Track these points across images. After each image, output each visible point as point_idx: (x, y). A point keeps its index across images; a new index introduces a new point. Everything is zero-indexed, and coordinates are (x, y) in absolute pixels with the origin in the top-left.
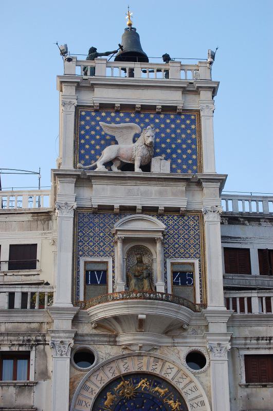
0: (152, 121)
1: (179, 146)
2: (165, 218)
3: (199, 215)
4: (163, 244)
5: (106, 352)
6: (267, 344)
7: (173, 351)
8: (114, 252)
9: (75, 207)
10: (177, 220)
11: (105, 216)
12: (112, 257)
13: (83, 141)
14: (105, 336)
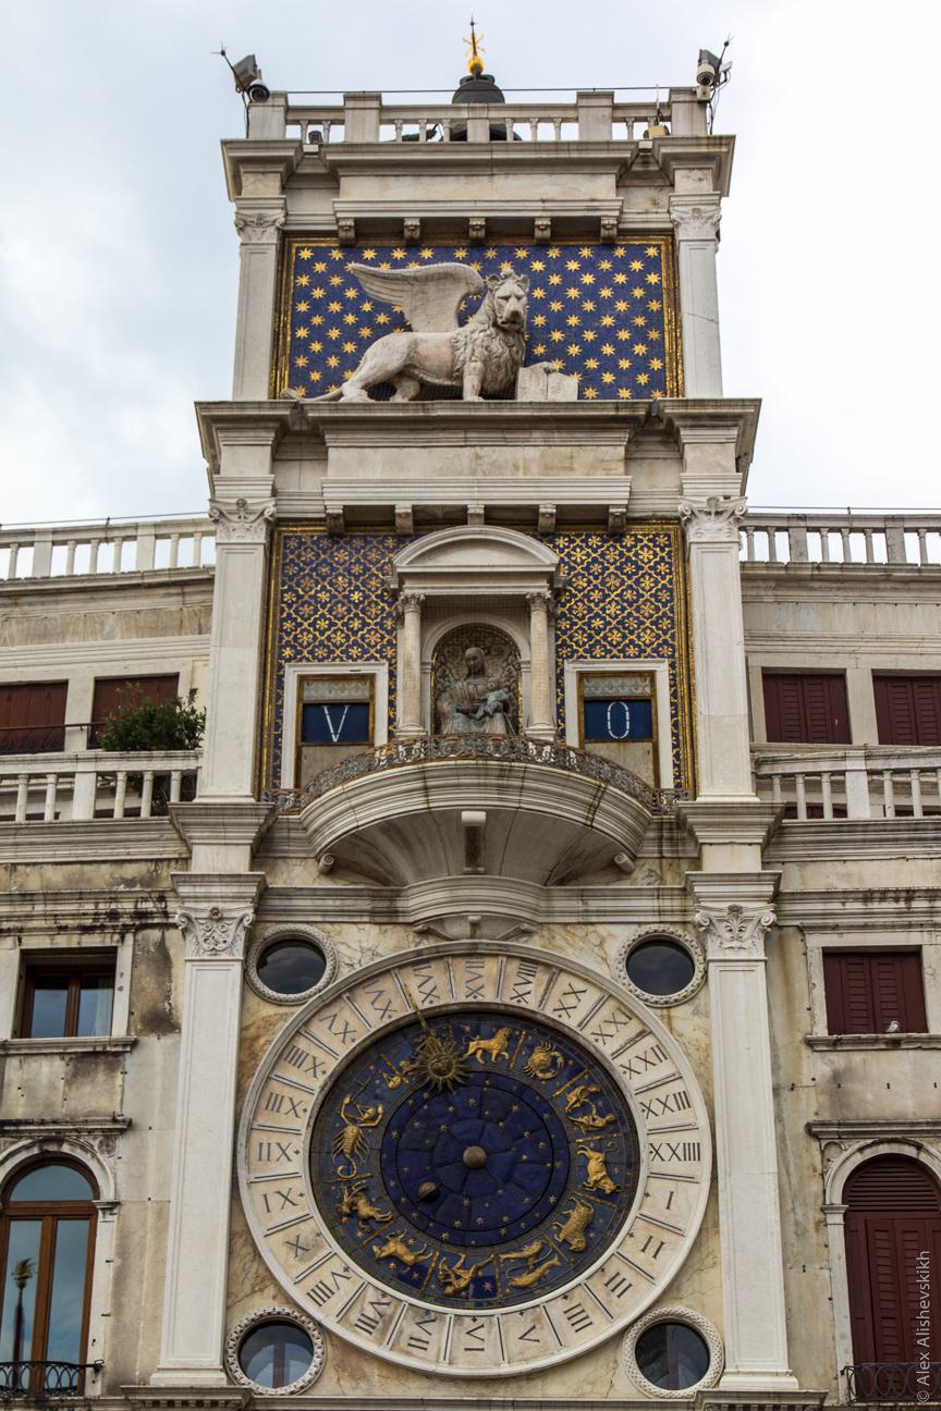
1: (607, 335)
2: (561, 542)
5: (363, 945)
7: (585, 939)
8: (394, 646)
11: (367, 542)
12: (389, 660)
13: (302, 333)
14: (357, 894)
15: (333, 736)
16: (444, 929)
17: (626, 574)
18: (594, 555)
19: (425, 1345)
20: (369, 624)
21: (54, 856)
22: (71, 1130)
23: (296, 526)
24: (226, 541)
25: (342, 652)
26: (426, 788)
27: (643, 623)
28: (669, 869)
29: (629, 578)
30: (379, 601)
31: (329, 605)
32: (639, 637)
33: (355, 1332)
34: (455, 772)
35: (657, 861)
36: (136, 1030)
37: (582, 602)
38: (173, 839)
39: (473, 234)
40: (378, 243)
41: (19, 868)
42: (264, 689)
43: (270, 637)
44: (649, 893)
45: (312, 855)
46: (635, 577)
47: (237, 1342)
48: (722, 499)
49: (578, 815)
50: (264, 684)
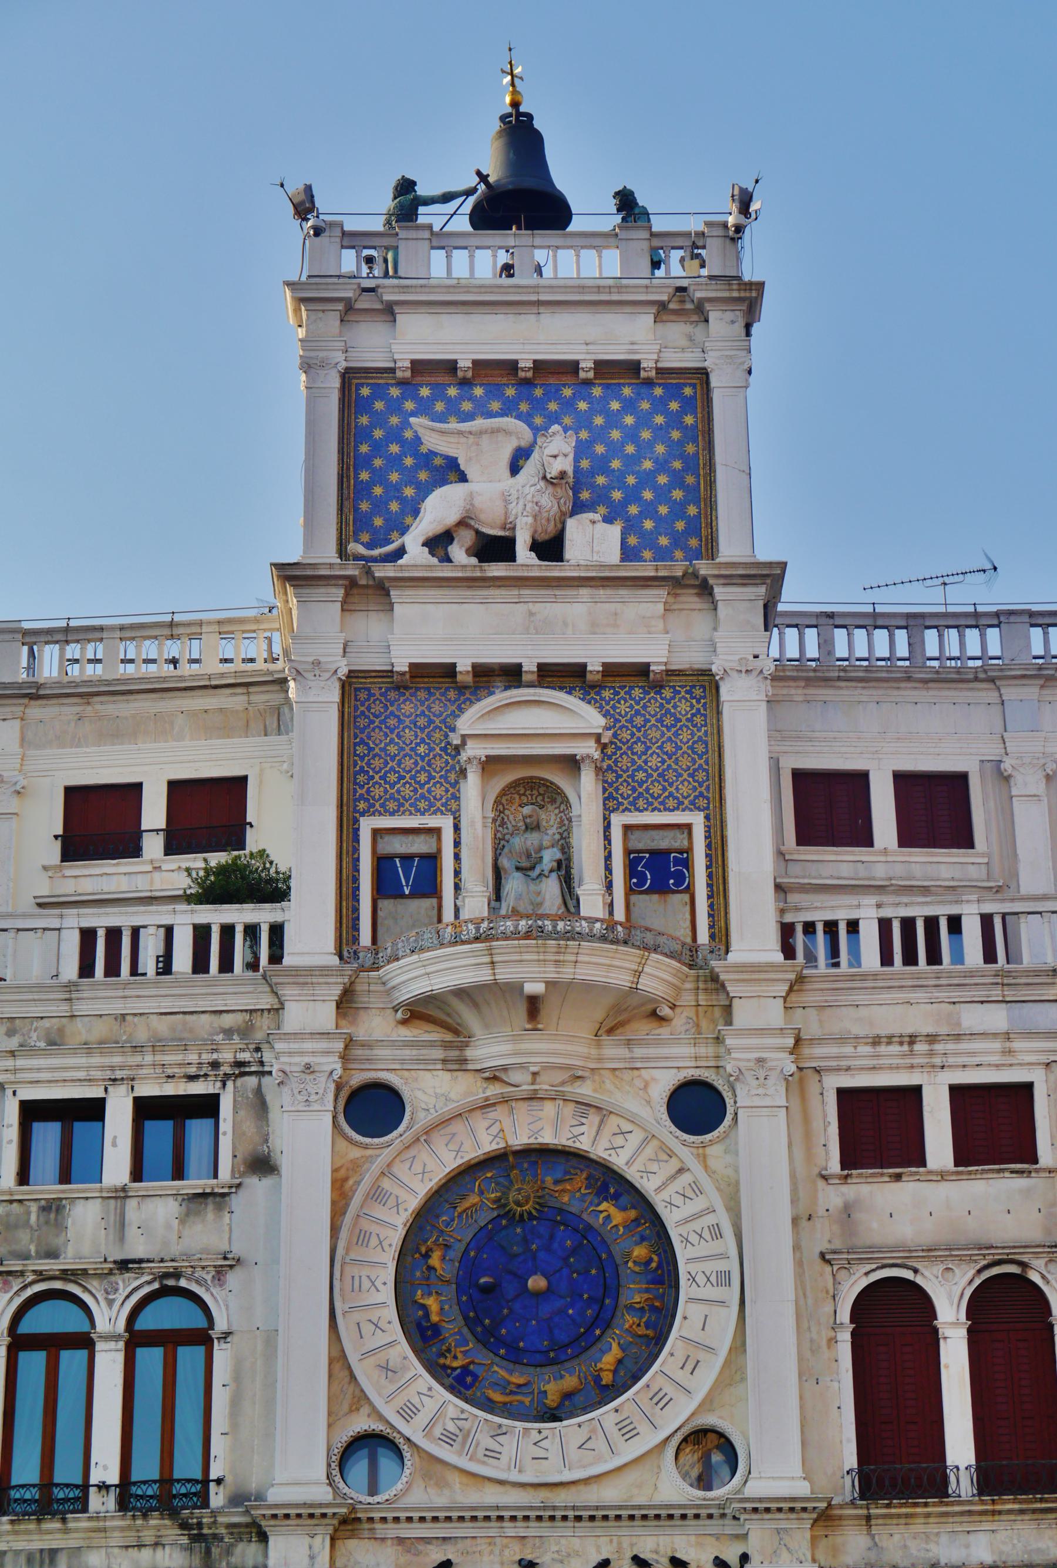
0: (568, 405)
1: (647, 480)
2: (607, 694)
3: (705, 683)
4: (598, 770)
5: (438, 1091)
6: (904, 1056)
8: (457, 799)
9: (343, 672)
10: (642, 699)
11: (430, 694)
12: (453, 813)
14: (431, 1044)
16: (508, 1077)
18: (637, 707)
19: (498, 1456)
21: (159, 1007)
22: (186, 1267)
23: (365, 678)
25: (410, 805)
26: (492, 963)
27: (681, 775)
29: (668, 730)
32: (677, 789)
33: (440, 1445)
34: (518, 950)
35: (694, 1008)
36: (239, 1172)
39: (522, 374)
40: (433, 380)
41: (128, 1018)
42: (341, 842)
43: (345, 791)
44: (687, 1041)
46: (673, 730)
47: (338, 1457)
48: (751, 658)
49: (624, 980)
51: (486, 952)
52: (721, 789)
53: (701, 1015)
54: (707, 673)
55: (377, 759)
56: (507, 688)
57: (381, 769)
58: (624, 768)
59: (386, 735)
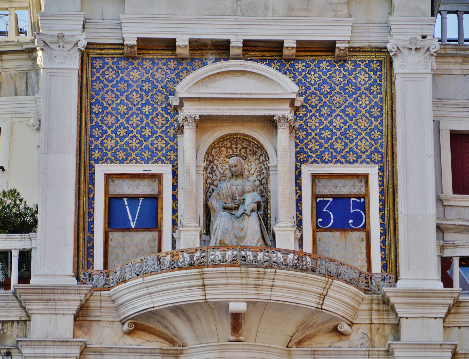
2: (299, 66)
4: (292, 128)
8: (175, 150)
9: (82, 44)
10: (328, 71)
12: (172, 162)
15: (132, 223)
17: (349, 94)
20: (157, 132)
23: (101, 49)
24: (49, 67)
25: (137, 155)
26: (204, 285)
28: (377, 333)
29: (350, 97)
30: (164, 113)
31: (126, 116)
34: (225, 275)
35: (368, 326)
37: (315, 116)
38: (16, 307)
44: (363, 353)
45: (119, 319)
46: (354, 96)
48: (420, 38)
50: (79, 180)
51: (199, 277)
52: (393, 145)
53: (374, 331)
54: (383, 50)
55: (109, 116)
56: (217, 60)
57: (113, 125)
58: (313, 127)
59: (117, 97)
